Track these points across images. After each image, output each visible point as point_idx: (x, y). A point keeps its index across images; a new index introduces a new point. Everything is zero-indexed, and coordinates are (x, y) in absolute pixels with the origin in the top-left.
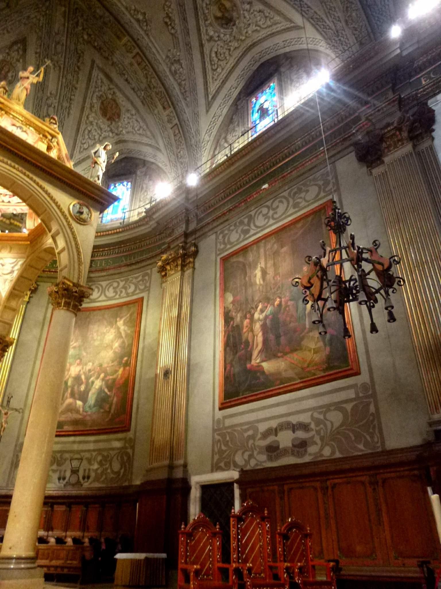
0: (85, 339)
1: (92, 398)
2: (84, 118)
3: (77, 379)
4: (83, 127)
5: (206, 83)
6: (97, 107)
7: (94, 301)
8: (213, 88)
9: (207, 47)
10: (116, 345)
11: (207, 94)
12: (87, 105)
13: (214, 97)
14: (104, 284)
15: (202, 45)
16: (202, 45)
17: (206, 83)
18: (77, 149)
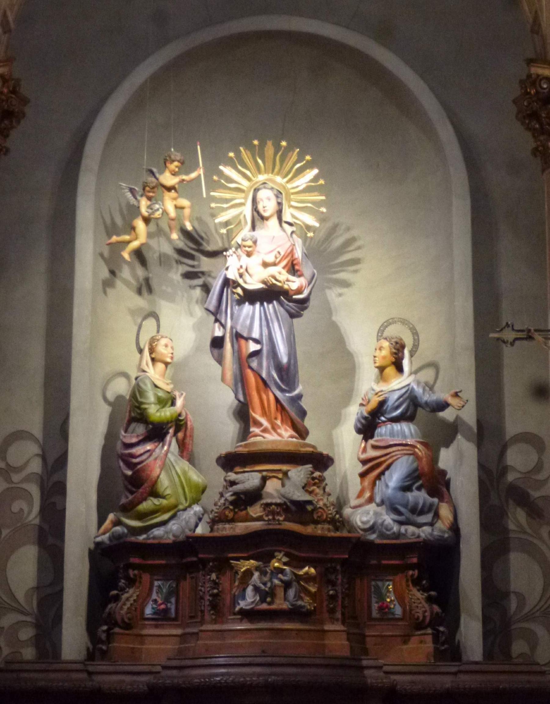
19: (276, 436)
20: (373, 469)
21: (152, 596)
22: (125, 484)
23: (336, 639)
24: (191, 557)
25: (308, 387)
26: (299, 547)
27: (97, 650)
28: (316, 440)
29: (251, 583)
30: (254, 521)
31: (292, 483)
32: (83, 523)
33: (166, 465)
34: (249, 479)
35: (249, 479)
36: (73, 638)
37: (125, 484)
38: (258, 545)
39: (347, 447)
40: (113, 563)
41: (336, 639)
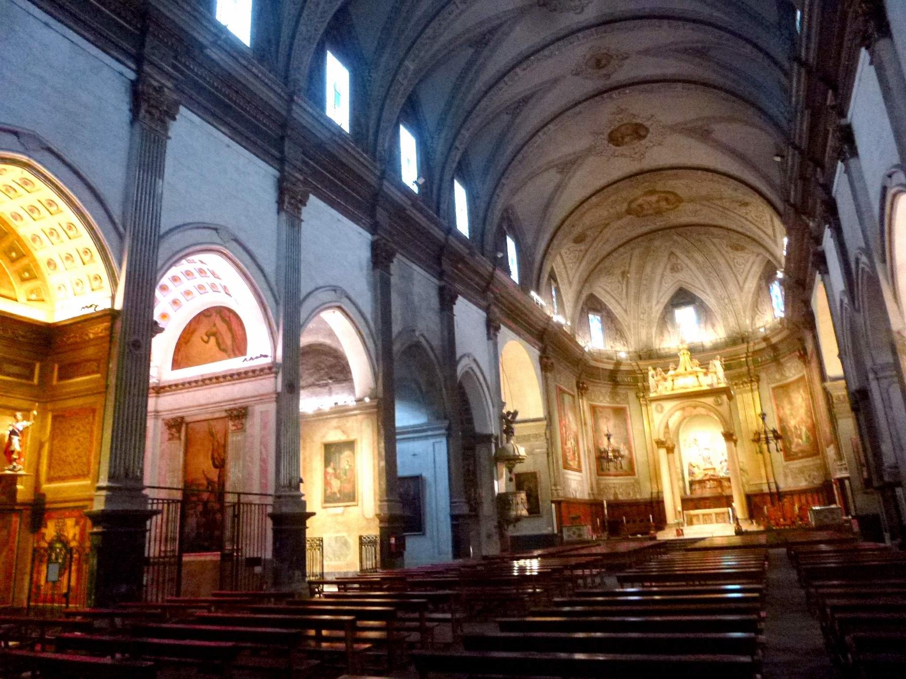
0: (791, 403)
1: (804, 438)
2: (728, 258)
3: (795, 427)
4: (731, 264)
5: (764, 232)
6: (729, 249)
7: (787, 378)
8: (770, 232)
9: (750, 218)
10: (804, 405)
11: (769, 237)
12: (724, 252)
13: (775, 236)
14: (788, 365)
15: (746, 219)
16: (746, 219)
17: (764, 232)
18: (739, 277)
19: (709, 466)
20: (722, 468)
21: (697, 486)
22: (691, 474)
23: (719, 490)
24: (701, 482)
25: (711, 460)
26: (714, 480)
27: (691, 493)
28: (714, 466)
29: (709, 484)
30: (707, 477)
31: (711, 472)
32: (687, 479)
33: (696, 470)
34: (706, 472)
35: (706, 472)
36: (688, 492)
37: (691, 474)
38: (709, 480)
39: (718, 467)
40: (692, 483)
41: (719, 490)
